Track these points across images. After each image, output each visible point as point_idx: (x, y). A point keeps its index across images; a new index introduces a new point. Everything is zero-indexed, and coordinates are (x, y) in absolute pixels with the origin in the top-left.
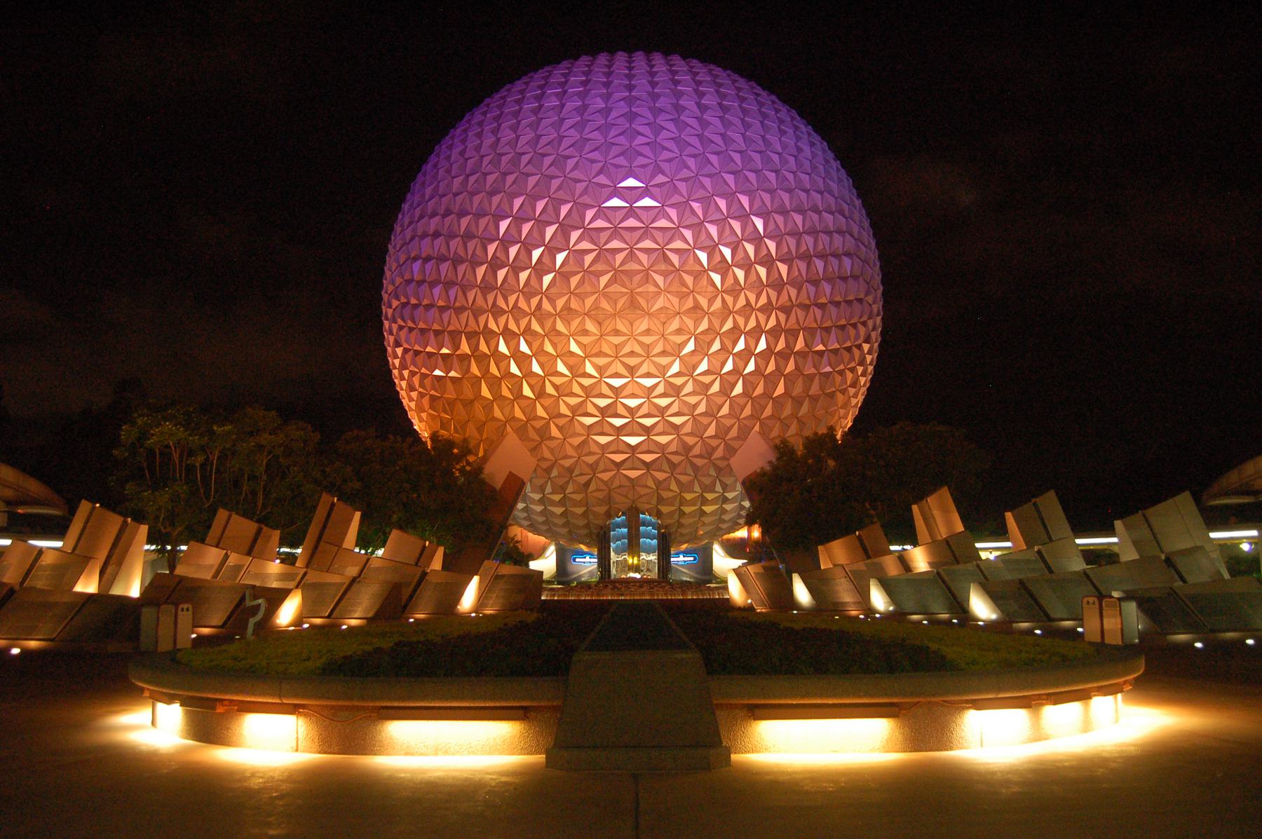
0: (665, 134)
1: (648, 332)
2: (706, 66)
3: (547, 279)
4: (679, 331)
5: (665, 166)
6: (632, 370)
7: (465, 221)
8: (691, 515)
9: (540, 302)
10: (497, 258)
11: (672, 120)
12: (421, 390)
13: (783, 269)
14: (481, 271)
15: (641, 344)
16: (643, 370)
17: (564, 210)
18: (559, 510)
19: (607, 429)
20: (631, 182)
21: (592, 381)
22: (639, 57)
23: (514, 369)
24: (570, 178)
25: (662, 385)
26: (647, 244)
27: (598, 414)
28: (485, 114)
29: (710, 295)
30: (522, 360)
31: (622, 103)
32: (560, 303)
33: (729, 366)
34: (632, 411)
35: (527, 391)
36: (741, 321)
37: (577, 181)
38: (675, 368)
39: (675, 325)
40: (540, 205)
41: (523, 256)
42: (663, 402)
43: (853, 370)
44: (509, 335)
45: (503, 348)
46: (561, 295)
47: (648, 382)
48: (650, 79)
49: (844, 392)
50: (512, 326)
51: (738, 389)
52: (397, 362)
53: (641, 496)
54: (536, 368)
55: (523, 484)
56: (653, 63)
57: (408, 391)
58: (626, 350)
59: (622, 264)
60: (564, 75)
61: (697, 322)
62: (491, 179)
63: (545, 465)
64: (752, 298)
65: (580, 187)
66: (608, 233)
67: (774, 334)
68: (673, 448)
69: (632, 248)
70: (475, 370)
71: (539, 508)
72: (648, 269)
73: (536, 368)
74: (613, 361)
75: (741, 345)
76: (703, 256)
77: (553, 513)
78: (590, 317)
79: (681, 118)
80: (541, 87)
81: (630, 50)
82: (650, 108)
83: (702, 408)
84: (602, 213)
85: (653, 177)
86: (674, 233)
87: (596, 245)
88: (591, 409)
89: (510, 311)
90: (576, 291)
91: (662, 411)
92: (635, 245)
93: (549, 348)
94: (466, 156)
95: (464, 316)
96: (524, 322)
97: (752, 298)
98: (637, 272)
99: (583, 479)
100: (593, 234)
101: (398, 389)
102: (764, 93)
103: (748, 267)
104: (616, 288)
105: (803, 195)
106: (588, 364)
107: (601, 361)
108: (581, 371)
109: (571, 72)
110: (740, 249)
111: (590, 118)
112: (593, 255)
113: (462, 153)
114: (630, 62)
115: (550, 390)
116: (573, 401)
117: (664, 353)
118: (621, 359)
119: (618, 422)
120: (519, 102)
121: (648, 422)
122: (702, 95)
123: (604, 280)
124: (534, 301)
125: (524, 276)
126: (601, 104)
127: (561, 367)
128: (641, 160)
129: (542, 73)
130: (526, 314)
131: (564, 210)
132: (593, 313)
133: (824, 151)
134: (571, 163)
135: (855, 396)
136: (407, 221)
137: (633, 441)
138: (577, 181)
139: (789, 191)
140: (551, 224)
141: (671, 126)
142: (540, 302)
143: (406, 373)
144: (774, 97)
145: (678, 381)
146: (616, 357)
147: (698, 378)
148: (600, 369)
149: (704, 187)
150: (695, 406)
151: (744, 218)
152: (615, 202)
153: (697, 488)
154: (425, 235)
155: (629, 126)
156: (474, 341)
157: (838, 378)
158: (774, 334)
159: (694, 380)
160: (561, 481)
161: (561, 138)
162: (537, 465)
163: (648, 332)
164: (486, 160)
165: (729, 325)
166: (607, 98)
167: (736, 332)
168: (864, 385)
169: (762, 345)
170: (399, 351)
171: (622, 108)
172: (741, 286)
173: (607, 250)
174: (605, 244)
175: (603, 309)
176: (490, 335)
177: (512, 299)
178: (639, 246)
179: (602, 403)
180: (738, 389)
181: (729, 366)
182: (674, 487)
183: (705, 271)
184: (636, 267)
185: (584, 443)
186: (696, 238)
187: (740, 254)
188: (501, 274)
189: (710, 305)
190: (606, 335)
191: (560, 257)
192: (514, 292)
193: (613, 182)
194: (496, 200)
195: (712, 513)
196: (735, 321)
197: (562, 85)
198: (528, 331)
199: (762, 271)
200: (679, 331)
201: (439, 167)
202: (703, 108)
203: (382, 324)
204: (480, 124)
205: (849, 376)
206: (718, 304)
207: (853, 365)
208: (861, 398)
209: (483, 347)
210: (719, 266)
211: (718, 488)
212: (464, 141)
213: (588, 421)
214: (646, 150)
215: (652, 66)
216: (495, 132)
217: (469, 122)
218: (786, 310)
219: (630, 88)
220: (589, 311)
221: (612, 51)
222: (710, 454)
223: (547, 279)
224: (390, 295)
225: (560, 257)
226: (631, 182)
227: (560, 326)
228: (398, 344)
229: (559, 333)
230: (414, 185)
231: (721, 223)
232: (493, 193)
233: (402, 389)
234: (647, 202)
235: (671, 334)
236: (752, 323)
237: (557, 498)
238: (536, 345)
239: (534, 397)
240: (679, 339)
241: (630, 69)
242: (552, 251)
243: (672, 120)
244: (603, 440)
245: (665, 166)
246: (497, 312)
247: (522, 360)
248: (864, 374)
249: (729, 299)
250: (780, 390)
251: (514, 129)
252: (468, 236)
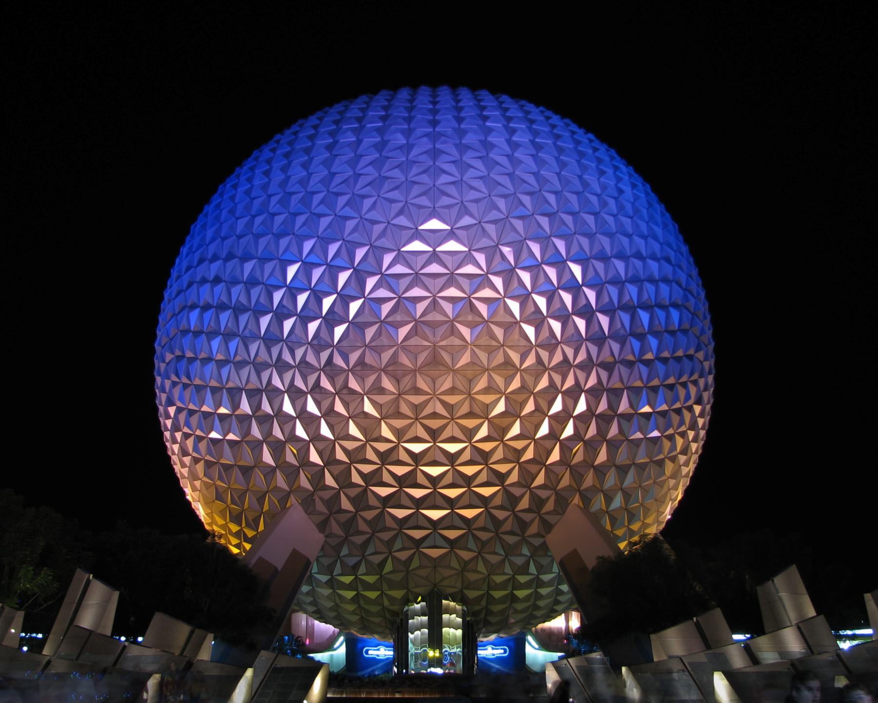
0: (471, 173)
1: (452, 391)
2: (517, 102)
3: (339, 331)
4: (487, 391)
5: (472, 207)
6: (434, 434)
7: (248, 267)
8: (502, 600)
9: (331, 357)
10: (284, 306)
11: (480, 158)
12: (195, 455)
13: (604, 320)
14: (265, 321)
15: (444, 404)
16: (446, 434)
17: (360, 253)
18: (350, 594)
20: (434, 224)
21: (389, 446)
22: (444, 93)
23: (300, 432)
24: (366, 219)
25: (468, 451)
26: (452, 292)
27: (393, 483)
28: (273, 150)
29: (523, 350)
30: (310, 422)
31: (425, 139)
32: (354, 357)
33: (544, 430)
34: (434, 481)
35: (314, 457)
36: (557, 379)
37: (374, 222)
38: (483, 432)
39: (482, 383)
40: (333, 249)
41: (313, 304)
43: (683, 435)
44: (296, 395)
45: (288, 407)
46: (354, 348)
47: (452, 448)
48: (456, 114)
49: (673, 459)
50: (299, 383)
51: (555, 456)
52: (169, 423)
53: (444, 579)
54: (325, 431)
55: (308, 564)
56: (460, 97)
57: (181, 455)
58: (428, 411)
59: (424, 314)
60: (361, 110)
61: (509, 380)
62: (279, 220)
63: (334, 542)
64: (570, 352)
65: (378, 229)
66: (409, 279)
67: (594, 394)
68: (480, 523)
69: (434, 296)
70: (256, 432)
71: (326, 592)
72: (453, 320)
73: (325, 431)
74: (412, 424)
75: (557, 406)
76: (514, 306)
78: (386, 373)
79: (491, 155)
80: (336, 122)
81: (434, 84)
82: (456, 145)
84: (401, 258)
85: (459, 218)
86: (483, 281)
87: (393, 292)
88: (387, 478)
89: (298, 366)
90: (373, 344)
91: (468, 481)
92: (440, 291)
93: (339, 407)
94: (252, 196)
95: (245, 372)
96: (312, 379)
97: (570, 352)
98: (443, 323)
99: (377, 559)
100: (392, 281)
101: (170, 453)
102: (581, 131)
103: (564, 318)
104: (415, 341)
105: (625, 241)
106: (383, 425)
107: (399, 423)
108: (375, 435)
109: (368, 107)
110: (556, 299)
111: (390, 155)
112: (391, 304)
113: (248, 192)
114: (434, 96)
115: (340, 455)
116: (366, 469)
117: (470, 415)
118: (422, 421)
119: (418, 493)
120: (312, 138)
121: (452, 493)
122: (513, 131)
123: (403, 332)
124: (325, 356)
125: (313, 327)
126: (402, 140)
127: (353, 430)
128: (446, 201)
129: (338, 107)
130: (313, 369)
131: (360, 253)
132: (389, 368)
133: (647, 194)
134: (367, 203)
135: (687, 464)
136: (185, 265)
137: (435, 515)
138: (374, 222)
139: (610, 235)
140: (345, 269)
141: (479, 164)
142: (331, 357)
143: (178, 435)
144: (591, 136)
145: (487, 447)
146: (417, 419)
147: (511, 443)
148: (399, 433)
149: (514, 229)
151: (560, 264)
152: (417, 246)
153: (508, 569)
154: (204, 281)
155: (432, 163)
157: (667, 444)
158: (594, 394)
159: (505, 445)
160: (352, 561)
161: (358, 176)
162: (325, 541)
163: (452, 391)
164: (274, 200)
165: (544, 383)
166: (407, 133)
167: (552, 391)
168: (696, 452)
169: (581, 406)
170: (172, 410)
171: (425, 144)
172: (557, 339)
173: (407, 299)
174: (404, 292)
175: (402, 364)
176: (274, 394)
177: (299, 353)
178: (442, 294)
179: (400, 471)
180: (555, 456)
181: (544, 430)
182: (481, 567)
183: (517, 323)
184: (439, 317)
186: (506, 285)
187: (556, 305)
188: (288, 324)
189: (522, 361)
190: (405, 393)
191: (354, 307)
192: (301, 344)
193: (414, 224)
194: (284, 242)
195: (527, 598)
196: (551, 379)
197: (359, 120)
198: (317, 388)
199: (581, 323)
200: (487, 391)
201: (221, 208)
202: (515, 146)
203: (153, 380)
204: (269, 162)
205: (680, 441)
206: (530, 360)
207: (683, 428)
208: (692, 466)
209: (266, 407)
210: (532, 317)
211: (532, 569)
212: (250, 180)
213: (384, 492)
214: (452, 190)
215: (458, 101)
216: (284, 169)
217: (256, 159)
218: (608, 367)
219: (434, 123)
220: (386, 366)
221: (414, 86)
223: (339, 331)
224: (163, 347)
225: (354, 307)
226: (434, 224)
227: (353, 384)
228: (170, 403)
229: (353, 392)
230: (195, 227)
231: (535, 269)
232: (279, 236)
233: (174, 453)
234: (452, 246)
235: (478, 393)
236: (570, 382)
237: (347, 579)
238: (326, 404)
239: (322, 464)
240: (487, 399)
241: (434, 103)
242: (345, 299)
243: (480, 158)
244: (401, 513)
245: (472, 207)
246: (282, 367)
247: (310, 422)
248: (695, 440)
249: (544, 355)
250: (602, 457)
251: (305, 166)
252: (252, 282)
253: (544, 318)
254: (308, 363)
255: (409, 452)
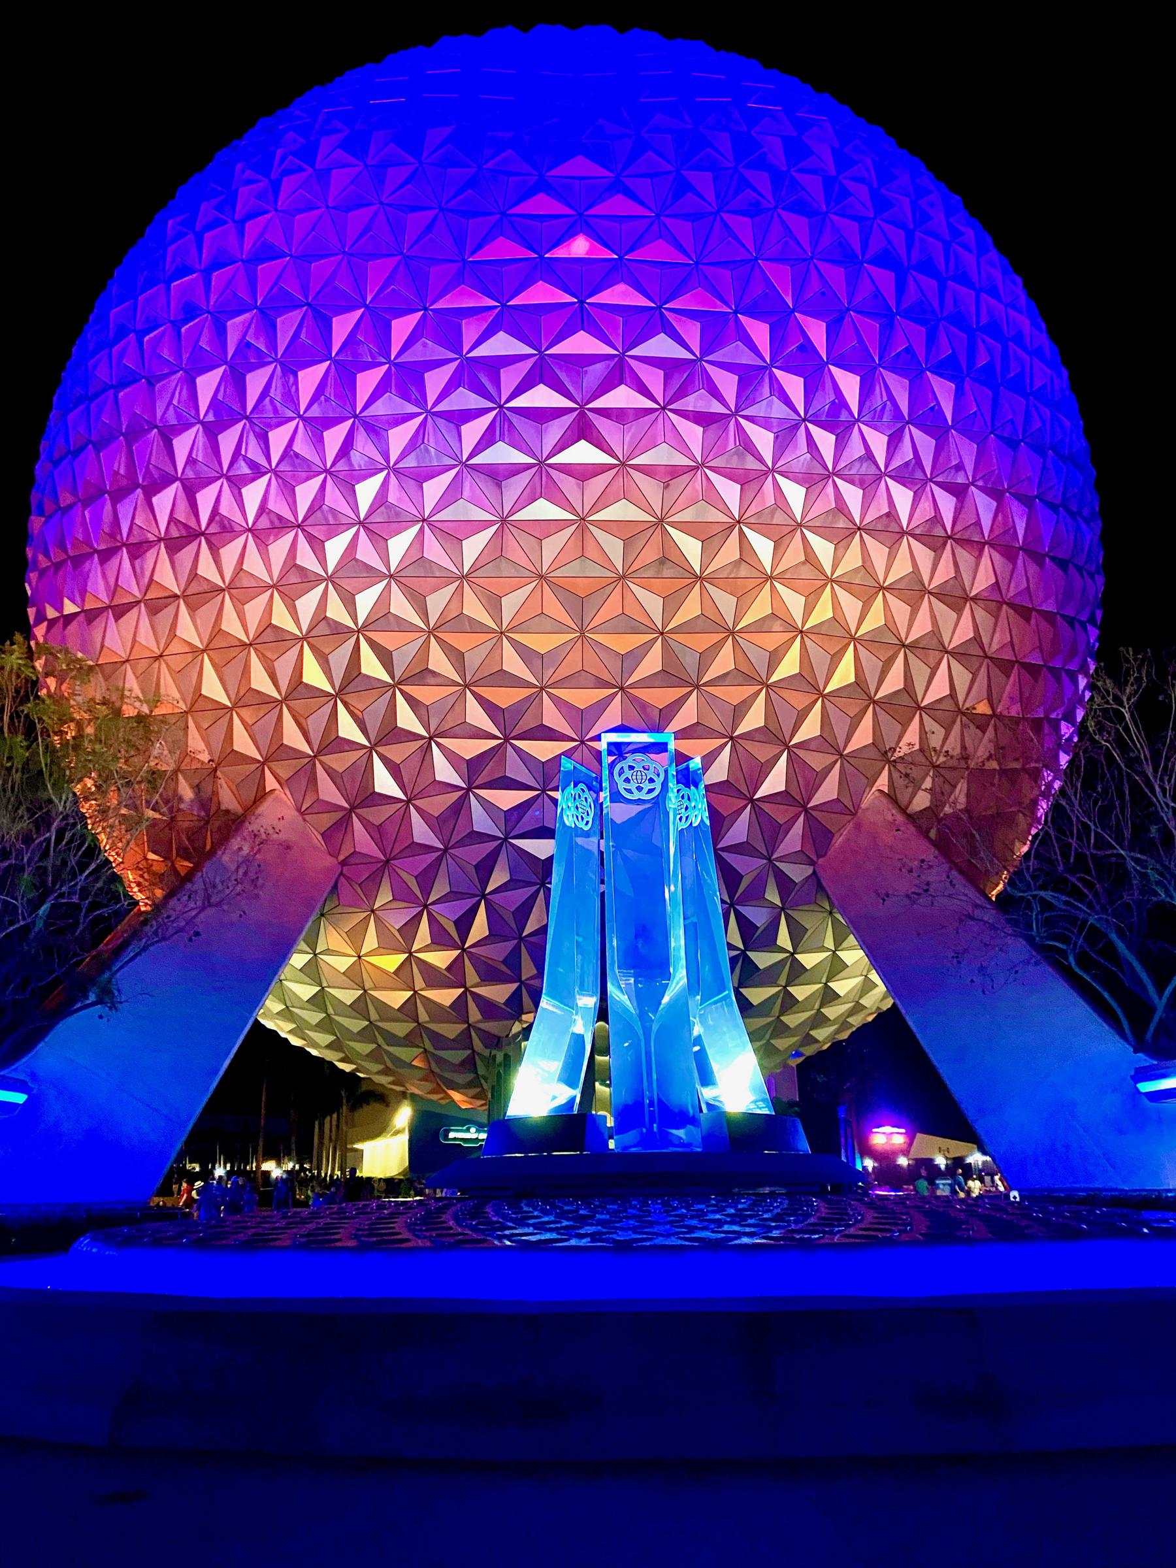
10: (248, 345)
19: (515, 769)
27: (490, 727)
42: (659, 697)
77: (382, 1007)
83: (754, 719)
119: (543, 750)
150: (739, 711)
156: (186, 554)
162: (341, 873)
185: (460, 808)
211: (784, 938)
222: (772, 844)
237: (391, 962)
244: (507, 799)
253: (823, 365)
254: (297, 455)
255: (525, 653)
